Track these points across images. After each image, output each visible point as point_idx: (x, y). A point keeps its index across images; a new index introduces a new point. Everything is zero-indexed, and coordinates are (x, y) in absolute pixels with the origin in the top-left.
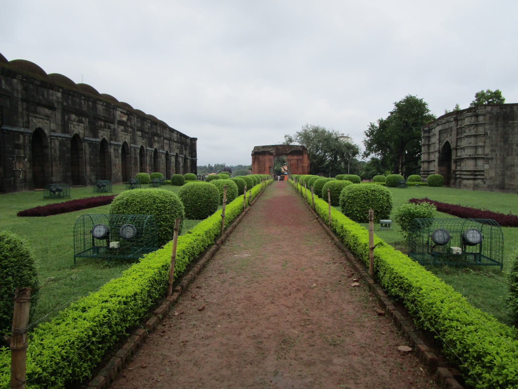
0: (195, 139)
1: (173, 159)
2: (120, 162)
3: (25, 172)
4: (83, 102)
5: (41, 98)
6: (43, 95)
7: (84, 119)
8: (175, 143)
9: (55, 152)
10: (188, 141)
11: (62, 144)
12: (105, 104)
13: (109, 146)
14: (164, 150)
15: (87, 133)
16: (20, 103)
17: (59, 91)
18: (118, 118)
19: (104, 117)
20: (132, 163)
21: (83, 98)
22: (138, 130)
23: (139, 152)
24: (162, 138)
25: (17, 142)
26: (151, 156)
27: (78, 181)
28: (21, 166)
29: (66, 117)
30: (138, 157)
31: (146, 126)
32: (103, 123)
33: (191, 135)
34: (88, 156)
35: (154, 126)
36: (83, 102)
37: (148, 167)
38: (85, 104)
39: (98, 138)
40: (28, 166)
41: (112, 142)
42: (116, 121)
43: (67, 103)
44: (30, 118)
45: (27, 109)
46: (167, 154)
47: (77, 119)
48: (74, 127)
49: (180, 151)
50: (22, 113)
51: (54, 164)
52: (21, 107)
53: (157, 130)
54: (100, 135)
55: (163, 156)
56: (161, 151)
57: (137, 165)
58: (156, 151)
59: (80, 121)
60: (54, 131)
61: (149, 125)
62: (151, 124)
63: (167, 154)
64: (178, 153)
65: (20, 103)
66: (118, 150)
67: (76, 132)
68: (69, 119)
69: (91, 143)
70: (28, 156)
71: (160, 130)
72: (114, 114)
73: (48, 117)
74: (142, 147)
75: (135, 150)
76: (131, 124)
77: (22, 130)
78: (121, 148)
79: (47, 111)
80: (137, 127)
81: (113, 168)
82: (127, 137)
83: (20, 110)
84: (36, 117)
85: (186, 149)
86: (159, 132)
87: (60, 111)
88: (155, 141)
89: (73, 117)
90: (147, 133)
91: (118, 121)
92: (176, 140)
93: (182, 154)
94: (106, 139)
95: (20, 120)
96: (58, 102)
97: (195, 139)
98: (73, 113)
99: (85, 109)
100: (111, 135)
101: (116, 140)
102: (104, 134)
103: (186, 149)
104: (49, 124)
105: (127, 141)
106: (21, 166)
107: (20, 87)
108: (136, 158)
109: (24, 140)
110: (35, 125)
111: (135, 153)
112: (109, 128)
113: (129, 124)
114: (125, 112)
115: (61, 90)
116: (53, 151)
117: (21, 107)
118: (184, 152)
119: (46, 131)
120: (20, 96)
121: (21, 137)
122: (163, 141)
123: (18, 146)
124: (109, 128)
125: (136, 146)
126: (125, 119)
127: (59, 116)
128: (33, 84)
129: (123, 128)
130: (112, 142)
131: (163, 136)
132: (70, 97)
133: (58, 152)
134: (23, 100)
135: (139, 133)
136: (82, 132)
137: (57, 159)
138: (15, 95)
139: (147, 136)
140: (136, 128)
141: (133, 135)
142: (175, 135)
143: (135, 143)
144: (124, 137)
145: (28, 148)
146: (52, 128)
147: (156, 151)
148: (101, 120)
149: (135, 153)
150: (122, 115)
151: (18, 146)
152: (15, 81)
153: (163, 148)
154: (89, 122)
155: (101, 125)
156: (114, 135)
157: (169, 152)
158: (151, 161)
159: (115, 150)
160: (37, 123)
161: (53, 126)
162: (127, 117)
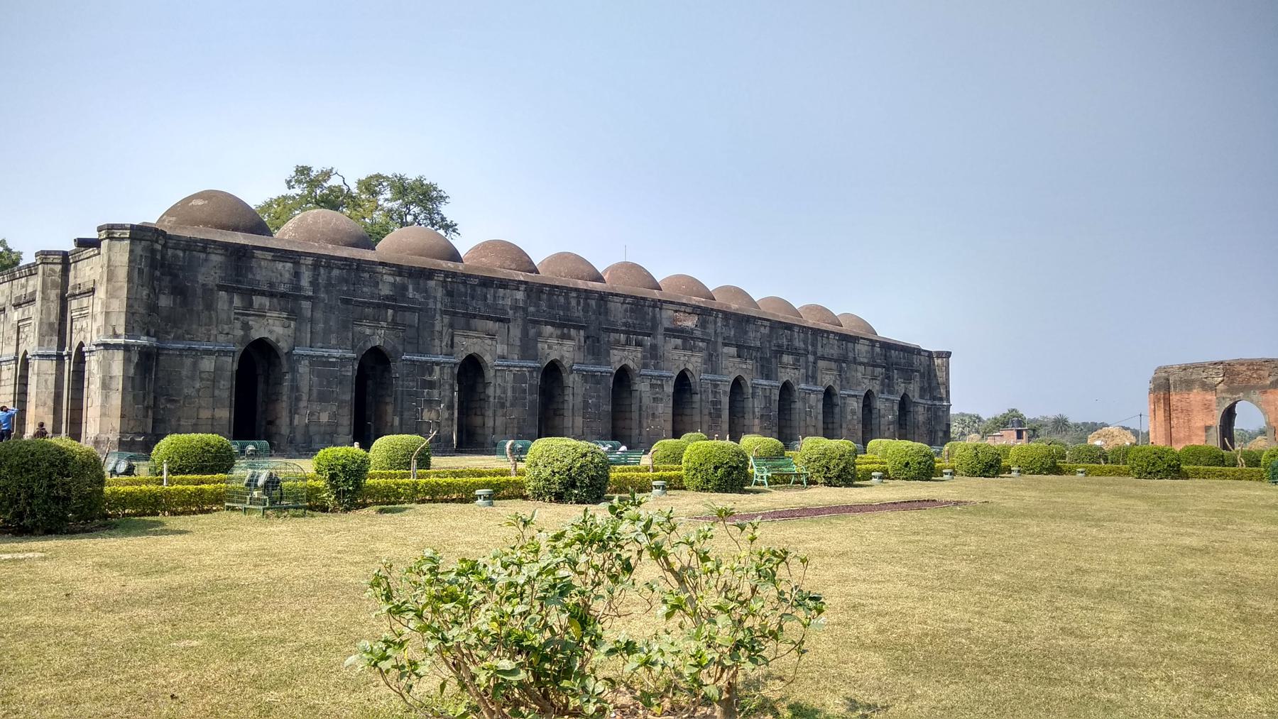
0: (948, 354)
1: (855, 405)
2: (670, 411)
3: (438, 424)
4: (573, 302)
5: (480, 304)
6: (485, 299)
7: (573, 332)
8: (861, 368)
9: (504, 392)
10: (924, 359)
11: (519, 378)
12: (628, 300)
13: (637, 379)
14: (816, 384)
15: (579, 356)
16: (438, 317)
17: (518, 289)
18: (667, 324)
19: (625, 324)
21: (574, 294)
22: (725, 345)
23: (728, 389)
24: (811, 358)
25: (428, 378)
26: (768, 399)
27: (470, 442)
28: (433, 415)
29: (532, 332)
30: (725, 400)
31: (751, 335)
33: (928, 344)
34: (579, 399)
36: (573, 302)
37: (757, 421)
38: (578, 303)
39: (609, 364)
40: (446, 415)
41: (643, 372)
42: (661, 330)
43: (537, 306)
44: (456, 339)
45: (451, 326)
46: (829, 393)
47: (559, 332)
48: (550, 347)
49: (882, 384)
50: (441, 333)
51: (500, 412)
52: (440, 323)
53: (791, 340)
55: (816, 401)
56: (803, 386)
58: (786, 388)
60: (503, 357)
61: (767, 331)
63: (829, 393)
64: (876, 387)
65: (438, 317)
66: (662, 386)
67: (554, 356)
68: (539, 334)
69: (589, 377)
70: (447, 399)
71: (805, 343)
72: (654, 317)
73: (492, 336)
75: (716, 386)
76: (704, 333)
77: (441, 359)
78: (672, 383)
79: (490, 324)
82: (693, 359)
83: (438, 327)
84: (467, 337)
85: (908, 380)
86: (798, 343)
87: (520, 321)
89: (549, 329)
90: (758, 349)
91: (667, 329)
93: (890, 392)
94: (631, 365)
95: (437, 342)
96: (515, 308)
97: (948, 354)
98: (547, 323)
99: (578, 312)
100: (644, 357)
101: (656, 367)
103: (908, 380)
104: (494, 348)
105: (690, 367)
106: (433, 415)
107: (440, 293)
108: (716, 403)
109: (442, 374)
110: (466, 349)
112: (639, 344)
113: (698, 333)
115: (523, 287)
116: (498, 391)
117: (440, 323)
118: (901, 388)
119: (487, 358)
120: (439, 306)
121: (437, 369)
122: (815, 363)
123: (431, 385)
125: (717, 377)
126: (690, 322)
127: (516, 332)
128: (464, 283)
129: (679, 342)
130: (643, 372)
131: (815, 353)
132: (545, 296)
133: (509, 393)
134: (445, 312)
135: (733, 350)
136: (567, 355)
137: (508, 404)
138: (431, 305)
140: (720, 340)
142: (862, 348)
143: (714, 372)
144: (677, 359)
145: (447, 387)
146: (499, 351)
147: (786, 388)
148: (617, 331)
149: (715, 393)
150: (680, 315)
151: (431, 385)
152: (432, 283)
153: (812, 378)
154: (587, 338)
156: (654, 354)
157: (837, 388)
159: (652, 386)
160: (469, 344)
161: (501, 349)
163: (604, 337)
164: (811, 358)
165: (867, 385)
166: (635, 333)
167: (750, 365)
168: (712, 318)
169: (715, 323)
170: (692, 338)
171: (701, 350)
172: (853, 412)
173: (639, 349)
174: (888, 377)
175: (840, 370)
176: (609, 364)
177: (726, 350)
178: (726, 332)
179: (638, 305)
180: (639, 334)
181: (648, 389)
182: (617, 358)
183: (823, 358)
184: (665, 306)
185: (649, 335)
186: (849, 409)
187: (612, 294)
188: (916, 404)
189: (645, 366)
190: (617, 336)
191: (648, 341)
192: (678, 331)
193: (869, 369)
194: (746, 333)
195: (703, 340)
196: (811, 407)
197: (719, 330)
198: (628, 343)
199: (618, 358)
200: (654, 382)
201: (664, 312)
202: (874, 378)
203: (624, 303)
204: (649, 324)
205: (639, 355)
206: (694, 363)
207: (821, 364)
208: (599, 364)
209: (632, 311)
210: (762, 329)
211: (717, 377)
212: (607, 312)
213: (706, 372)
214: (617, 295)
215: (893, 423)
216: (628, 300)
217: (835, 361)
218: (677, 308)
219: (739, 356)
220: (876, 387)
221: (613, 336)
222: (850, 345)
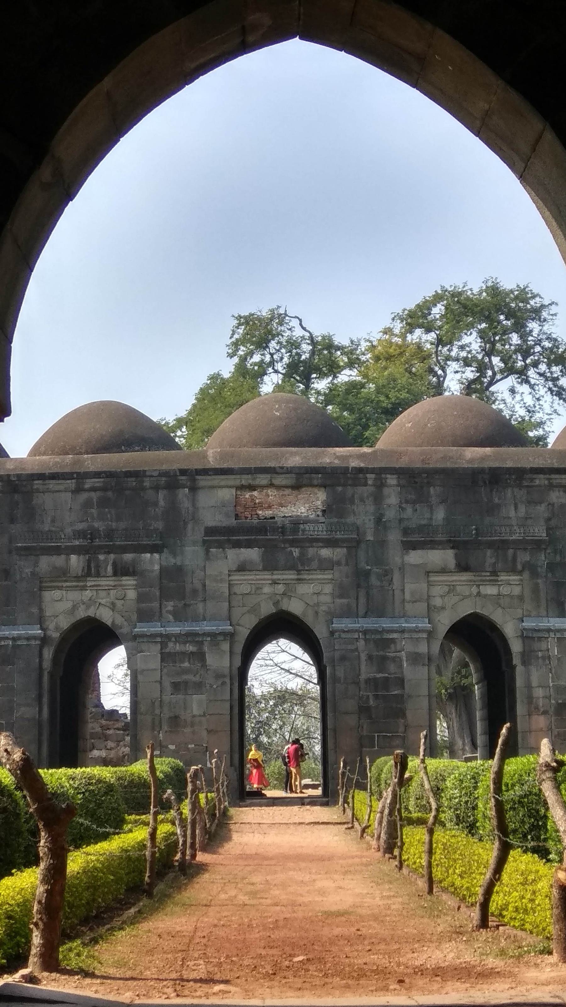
12: (89, 483)
18: (212, 519)
32: (75, 562)
41: (142, 628)
42: (195, 534)
66: (200, 656)
80: (406, 532)
82: (304, 589)
91: (210, 531)
100: (141, 598)
101: (179, 616)
112: (121, 571)
125: (385, 623)
126: (304, 507)
129: (253, 554)
130: (142, 628)
139: (542, 559)
140: (394, 537)
148: (57, 551)
149: (381, 662)
159: (165, 657)
162: (320, 498)
163: (24, 567)
166: (109, 550)
167: (512, 585)
168: (366, 491)
169: (378, 498)
170: (294, 543)
171: (327, 565)
173: (129, 581)
176: (41, 621)
177: (415, 557)
178: (414, 516)
179: (120, 488)
180: (124, 549)
181: (155, 663)
184: (202, 481)
185: (154, 549)
187: (41, 477)
189: (144, 616)
190: (59, 561)
191: (152, 562)
192: (250, 530)
195: (331, 543)
197: (390, 514)
198: (91, 571)
199: (62, 608)
200: (172, 647)
201: (205, 499)
203: (78, 490)
204: (160, 525)
205: (132, 594)
208: (13, 623)
209: (103, 503)
211: (385, 623)
212: (31, 514)
213: (348, 613)
214: (54, 476)
216: (89, 483)
218: (245, 480)
219: (463, 567)
221: (46, 563)
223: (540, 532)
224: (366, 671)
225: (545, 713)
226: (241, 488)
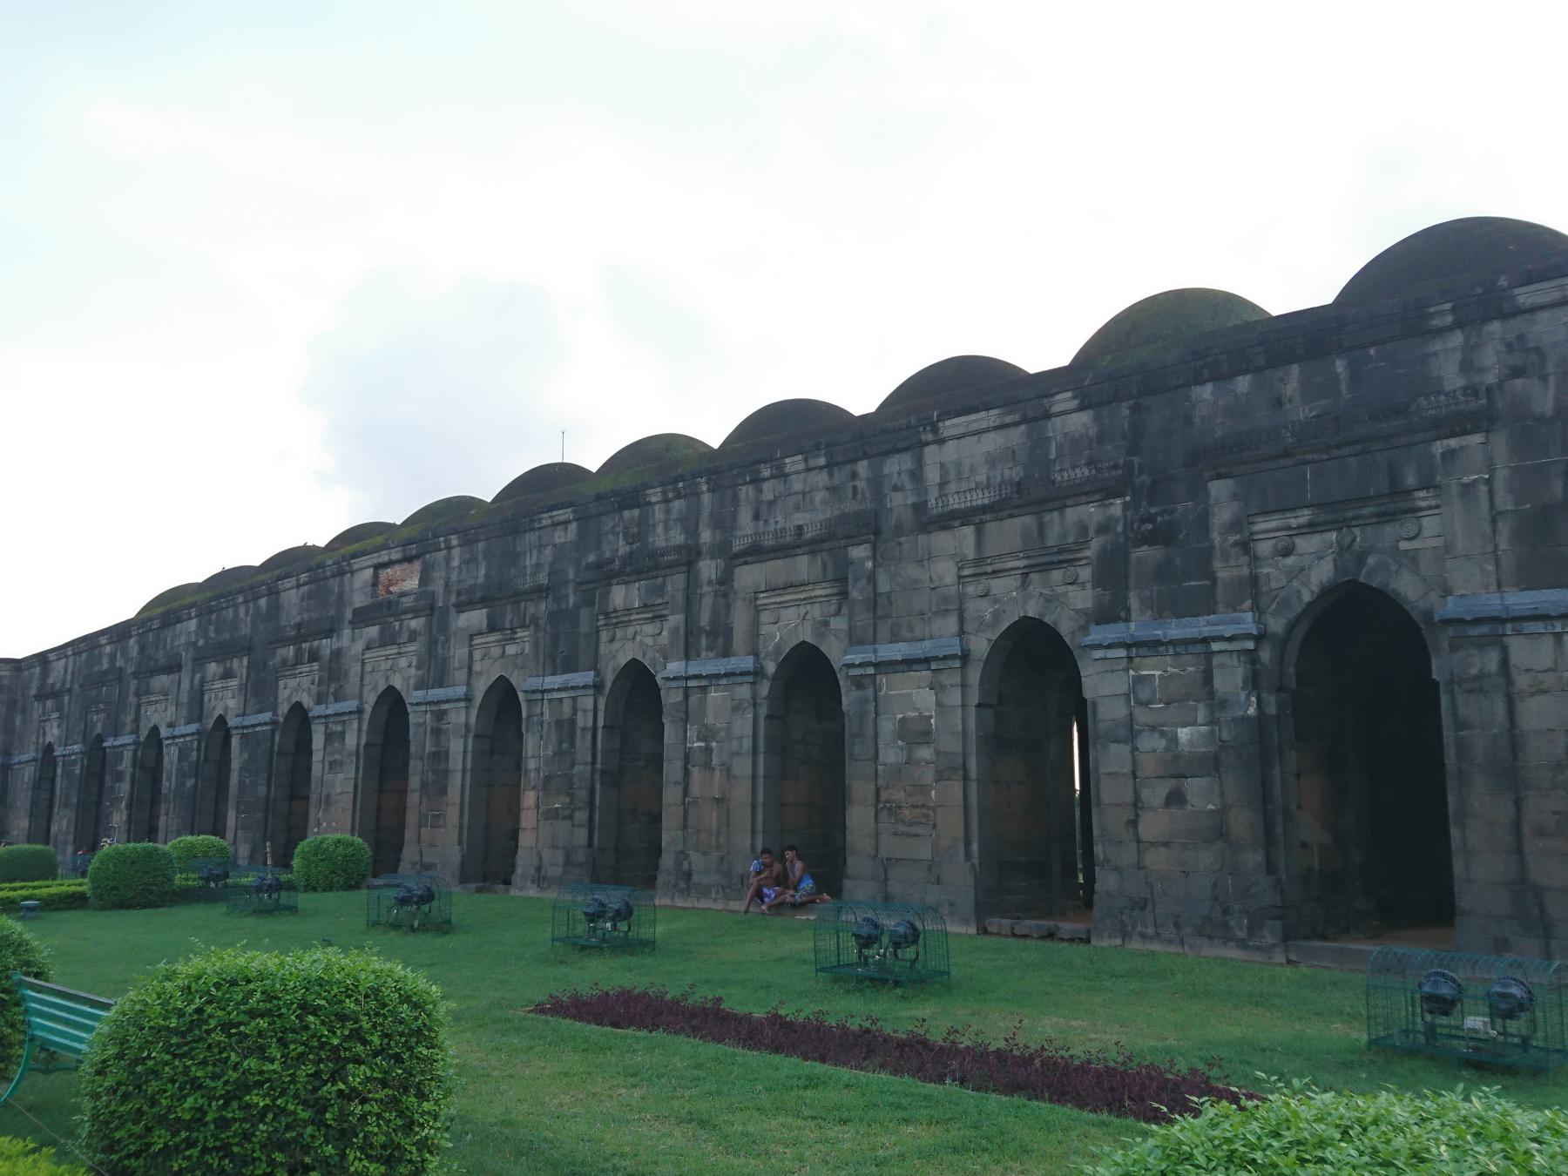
12: (304, 577)
20: (414, 782)
22: (461, 607)
26: (566, 728)
35: (609, 522)
38: (247, 614)
54: (283, 694)
56: (675, 667)
57: (443, 791)
58: (638, 685)
59: (228, 675)
62: (583, 519)
74: (392, 702)
75: (440, 716)
81: (314, 813)
82: (403, 662)
88: (615, 619)
92: (981, 499)
102: (296, 689)
105: (397, 682)
108: (440, 756)
111: (437, 732)
112: (314, 657)
114: (396, 555)
122: (725, 579)
124: (314, 657)
135: (476, 618)
139: (542, 608)
141: (432, 643)
155: (284, 662)
156: (334, 672)
157: (837, 653)
158: (564, 753)
164: (708, 569)
165: (1008, 600)
171: (413, 636)
172: (915, 733)
174: (1162, 536)
175: (840, 579)
182: (287, 693)
183: (756, 553)
186: (887, 727)
188: (1495, 628)
189: (320, 700)
191: (326, 646)
193: (1008, 533)
194: (514, 559)
196: (707, 734)
197: (454, 577)
202: (1046, 559)
206: (400, 669)
207: (748, 576)
210: (559, 537)
215: (1210, 764)
217: (813, 547)
219: (492, 628)
220: (1068, 601)
222: (896, 466)
223: (543, 579)
224: (429, 747)
225: (534, 788)
226: (378, 567)
